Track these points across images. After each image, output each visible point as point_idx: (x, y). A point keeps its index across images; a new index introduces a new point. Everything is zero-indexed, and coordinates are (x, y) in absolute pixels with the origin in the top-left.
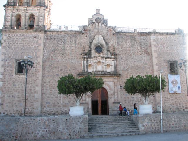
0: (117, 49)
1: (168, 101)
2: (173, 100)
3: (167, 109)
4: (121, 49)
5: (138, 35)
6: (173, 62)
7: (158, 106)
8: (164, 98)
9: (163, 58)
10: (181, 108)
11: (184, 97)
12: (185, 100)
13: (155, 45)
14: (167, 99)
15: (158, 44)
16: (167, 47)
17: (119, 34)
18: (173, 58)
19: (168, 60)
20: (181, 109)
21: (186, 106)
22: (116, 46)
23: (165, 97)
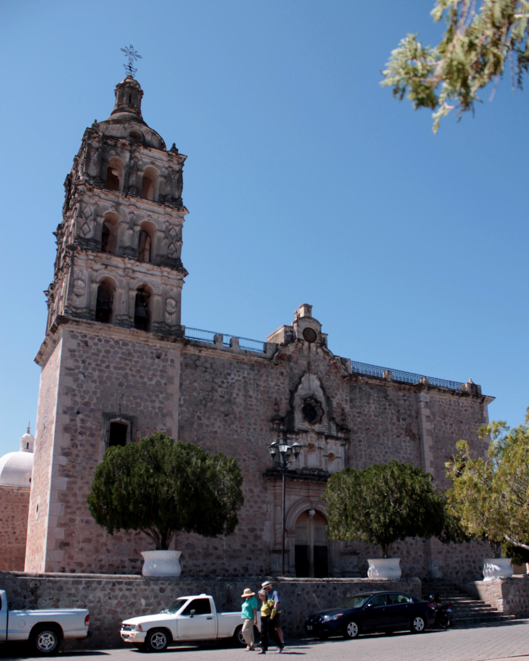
0: (350, 418)
1: (453, 553)
3: (451, 573)
4: (359, 417)
9: (444, 451)
15: (433, 414)
17: (354, 379)
22: (347, 407)
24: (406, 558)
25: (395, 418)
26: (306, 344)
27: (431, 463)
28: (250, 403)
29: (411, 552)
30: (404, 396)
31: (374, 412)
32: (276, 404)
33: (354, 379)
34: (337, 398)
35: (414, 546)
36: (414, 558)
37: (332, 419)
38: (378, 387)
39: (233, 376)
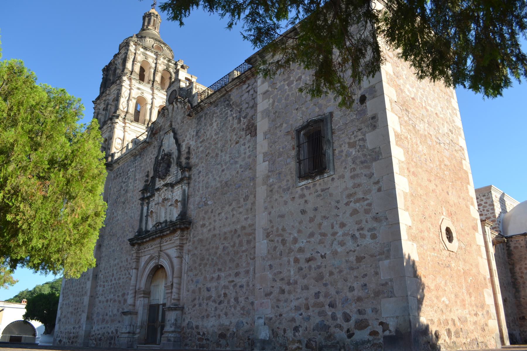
0: (193, 153)
1: (290, 292)
2: (306, 288)
4: (201, 147)
6: (315, 122)
7: (259, 318)
8: (279, 284)
9: (285, 125)
10: (336, 327)
11: (352, 269)
12: (355, 285)
13: (267, 91)
14: (289, 284)
16: (300, 78)
17: (199, 109)
18: (317, 110)
19: (300, 123)
20: (338, 330)
21: (360, 312)
22: (192, 143)
23: (282, 279)
24: (233, 309)
25: (236, 121)
26: (170, 108)
27: (265, 154)
29: (240, 299)
31: (215, 130)
32: (147, 176)
33: (199, 109)
34: (186, 139)
35: (244, 290)
36: (243, 308)
37: (179, 164)
38: (222, 99)
39: (131, 170)
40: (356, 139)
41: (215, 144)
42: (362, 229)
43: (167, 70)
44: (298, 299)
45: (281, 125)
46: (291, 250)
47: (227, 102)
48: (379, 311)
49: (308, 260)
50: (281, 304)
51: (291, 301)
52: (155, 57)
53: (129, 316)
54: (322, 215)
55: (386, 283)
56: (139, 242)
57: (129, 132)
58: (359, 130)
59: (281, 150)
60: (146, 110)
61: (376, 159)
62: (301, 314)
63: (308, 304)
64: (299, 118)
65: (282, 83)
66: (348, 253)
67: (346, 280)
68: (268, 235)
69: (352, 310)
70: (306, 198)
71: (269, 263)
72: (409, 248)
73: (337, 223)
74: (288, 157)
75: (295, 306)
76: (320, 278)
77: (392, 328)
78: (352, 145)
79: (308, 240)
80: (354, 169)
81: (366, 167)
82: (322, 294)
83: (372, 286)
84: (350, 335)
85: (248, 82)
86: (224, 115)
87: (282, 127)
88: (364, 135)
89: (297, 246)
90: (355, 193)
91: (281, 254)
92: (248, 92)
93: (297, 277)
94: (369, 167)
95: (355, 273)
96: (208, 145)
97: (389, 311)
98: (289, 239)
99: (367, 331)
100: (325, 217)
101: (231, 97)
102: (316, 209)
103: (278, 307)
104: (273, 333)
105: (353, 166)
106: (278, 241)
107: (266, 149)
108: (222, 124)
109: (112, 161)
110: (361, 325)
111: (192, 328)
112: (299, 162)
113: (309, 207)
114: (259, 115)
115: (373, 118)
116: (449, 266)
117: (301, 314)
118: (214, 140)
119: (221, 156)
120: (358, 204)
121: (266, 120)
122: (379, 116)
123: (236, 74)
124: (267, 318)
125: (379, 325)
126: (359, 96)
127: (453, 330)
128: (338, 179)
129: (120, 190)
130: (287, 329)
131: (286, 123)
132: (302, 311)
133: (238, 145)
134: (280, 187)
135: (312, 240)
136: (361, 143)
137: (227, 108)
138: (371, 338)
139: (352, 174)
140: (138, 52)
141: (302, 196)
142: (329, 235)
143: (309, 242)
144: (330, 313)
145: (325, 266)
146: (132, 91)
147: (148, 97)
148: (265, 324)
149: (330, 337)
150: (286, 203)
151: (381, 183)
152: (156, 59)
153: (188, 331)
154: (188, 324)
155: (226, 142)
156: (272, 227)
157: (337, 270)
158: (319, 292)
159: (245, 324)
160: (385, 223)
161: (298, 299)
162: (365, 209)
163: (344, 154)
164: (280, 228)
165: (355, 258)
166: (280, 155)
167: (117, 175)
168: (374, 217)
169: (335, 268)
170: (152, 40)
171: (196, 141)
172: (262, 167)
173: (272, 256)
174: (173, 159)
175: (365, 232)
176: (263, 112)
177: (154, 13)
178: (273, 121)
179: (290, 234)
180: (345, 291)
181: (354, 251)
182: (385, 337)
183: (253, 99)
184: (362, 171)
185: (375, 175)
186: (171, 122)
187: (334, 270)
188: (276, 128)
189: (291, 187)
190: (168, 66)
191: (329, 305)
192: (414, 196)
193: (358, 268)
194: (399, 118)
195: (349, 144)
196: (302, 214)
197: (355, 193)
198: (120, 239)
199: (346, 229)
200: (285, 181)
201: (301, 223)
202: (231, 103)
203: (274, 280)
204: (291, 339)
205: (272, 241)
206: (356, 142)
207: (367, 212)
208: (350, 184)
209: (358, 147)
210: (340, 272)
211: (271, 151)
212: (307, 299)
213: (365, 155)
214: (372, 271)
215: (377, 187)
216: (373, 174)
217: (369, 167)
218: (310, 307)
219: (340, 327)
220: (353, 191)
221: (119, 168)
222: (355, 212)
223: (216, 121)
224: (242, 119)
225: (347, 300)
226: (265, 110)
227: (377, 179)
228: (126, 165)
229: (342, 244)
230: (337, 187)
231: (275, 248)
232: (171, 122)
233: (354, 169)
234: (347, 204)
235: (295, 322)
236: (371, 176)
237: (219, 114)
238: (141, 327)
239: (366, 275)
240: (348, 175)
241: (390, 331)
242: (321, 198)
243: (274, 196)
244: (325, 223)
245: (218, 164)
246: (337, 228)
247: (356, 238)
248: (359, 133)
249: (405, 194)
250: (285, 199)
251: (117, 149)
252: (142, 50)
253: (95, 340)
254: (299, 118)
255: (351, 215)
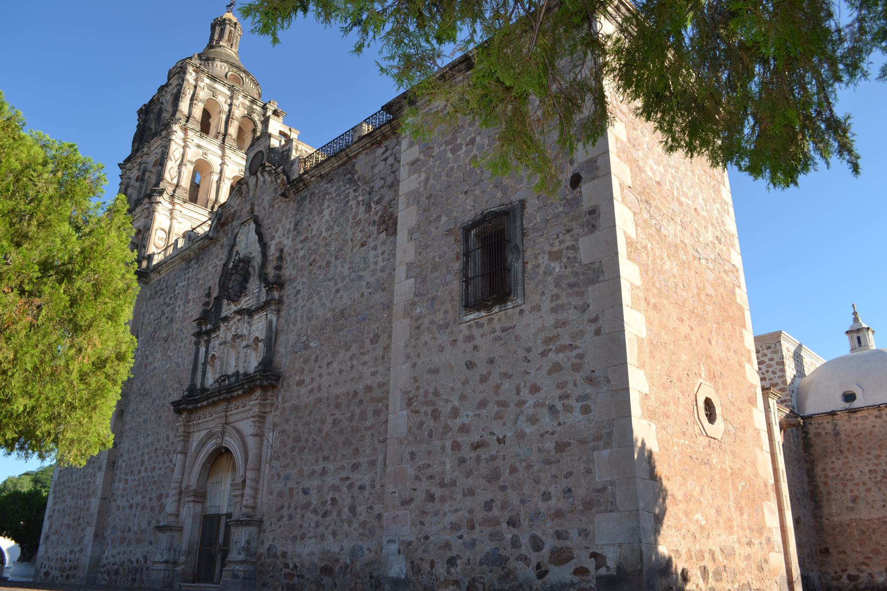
0: (288, 258)
1: (443, 500)
2: (471, 492)
3: (432, 564)
5: (365, 148)
6: (496, 215)
8: (425, 485)
9: (444, 219)
10: (518, 559)
11: (548, 462)
12: (552, 490)
13: (417, 160)
14: (442, 485)
15: (427, 149)
16: (473, 141)
17: (301, 184)
20: (521, 564)
21: (559, 535)
22: (287, 242)
23: (431, 477)
24: (346, 525)
25: (362, 208)
27: (410, 266)
28: (187, 310)
29: (359, 509)
30: (386, 150)
31: (327, 221)
32: (208, 295)
33: (301, 184)
34: (277, 235)
35: (366, 494)
36: (363, 524)
37: (263, 277)
38: (341, 170)
40: (563, 246)
41: (326, 245)
42: (567, 396)
43: (248, 117)
44: (456, 511)
45: (439, 218)
46: (447, 429)
47: (349, 176)
48: (591, 534)
49: (476, 446)
50: (428, 519)
51: (445, 514)
52: (229, 93)
53: (168, 533)
54: (502, 370)
55: (604, 488)
56: (190, 407)
57: (180, 219)
58: (568, 231)
59: (437, 259)
60: (210, 182)
61: (593, 281)
62: (461, 537)
63: (472, 520)
64: (469, 207)
65: (443, 148)
66: (542, 435)
67: (537, 482)
68: (409, 403)
69: (546, 531)
70: (475, 343)
71: (411, 448)
72: (644, 430)
73: (525, 386)
74: (449, 272)
75: (451, 523)
76: (494, 476)
77: (611, 563)
78: (555, 256)
79: (477, 412)
80: (557, 296)
81: (577, 294)
82: (497, 503)
83: (580, 492)
84: (542, 573)
85: (386, 143)
86: (342, 197)
87: (440, 221)
88: (576, 240)
89: (458, 421)
90: (558, 337)
91: (430, 435)
92: (385, 160)
93: (456, 474)
94: (581, 294)
95: (553, 470)
96: (314, 247)
97: (607, 537)
98: (446, 410)
99: (571, 566)
100: (506, 375)
101: (356, 168)
102: (491, 361)
103: (422, 523)
104: (413, 568)
105: (555, 291)
106: (426, 413)
107: (411, 257)
108: (339, 212)
109: (148, 267)
110: (561, 557)
111: (275, 556)
112: (467, 281)
113: (481, 357)
114: (402, 200)
115: (592, 212)
116: (707, 463)
117: (461, 537)
118: (325, 239)
119: (336, 267)
120: (561, 355)
121: (414, 208)
122: (602, 210)
123: (366, 129)
124: (402, 542)
125: (590, 557)
126: (570, 175)
127: (711, 569)
128: (530, 312)
129: (160, 318)
130: (436, 561)
131: (447, 215)
132: (462, 531)
133: (364, 248)
134: (432, 322)
135: (484, 412)
136: (571, 253)
137: (348, 186)
138: (576, 579)
139: (554, 304)
140: (201, 84)
141: (470, 338)
142: (512, 406)
143: (479, 416)
144: (509, 536)
145: (504, 456)
146: (188, 149)
147: (215, 161)
148: (399, 553)
149: (508, 576)
150: (441, 349)
151: (601, 321)
152: (231, 98)
153: (268, 561)
154: (269, 549)
155: (345, 242)
156: (418, 388)
157: (524, 464)
158: (492, 501)
159: (366, 552)
160: (605, 388)
161: (456, 511)
162: (573, 365)
163: (541, 270)
164: (431, 390)
165: (554, 445)
166: (435, 268)
167: (156, 292)
168: (587, 378)
169: (521, 461)
170: (226, 65)
171: (293, 240)
172: (404, 288)
173: (416, 438)
174: (254, 267)
175: (572, 402)
176: (408, 195)
177: (230, 20)
178: (424, 211)
179: (447, 401)
180: (536, 500)
181: (553, 434)
182: (599, 578)
183: (393, 172)
184: (570, 300)
185: (591, 308)
186: (253, 205)
187: (518, 465)
188: (430, 222)
189: (451, 324)
190: (251, 111)
191: (508, 523)
192: (653, 345)
193: (558, 461)
194: (635, 214)
195: (550, 253)
196: (468, 368)
197: (558, 337)
198: (158, 401)
199: (541, 395)
200: (442, 312)
201: (465, 382)
202: (356, 177)
203: (417, 478)
204: (442, 579)
205: (416, 412)
206: (561, 251)
207: (576, 368)
208: (550, 320)
209: (565, 260)
210: (529, 467)
211: (419, 261)
212: (471, 512)
213: (576, 274)
214: (582, 467)
215: (594, 327)
216: (588, 306)
217: (581, 294)
218: (476, 525)
219: (525, 559)
220: (555, 332)
221: (160, 280)
222: (556, 368)
223: (329, 206)
224: (373, 205)
225: (537, 514)
226: (413, 191)
227: (594, 315)
228: (172, 274)
229: (533, 420)
230: (528, 325)
231: (421, 424)
232: (253, 205)
233: (557, 296)
234: (544, 354)
235: (450, 549)
236: (584, 308)
237: (334, 195)
238: (189, 552)
239: (570, 474)
240: (546, 305)
241: (608, 567)
242: (501, 342)
243: (422, 337)
244: (506, 385)
245: (330, 280)
246: (525, 393)
247: (557, 412)
248: (568, 237)
249: (640, 341)
250: (440, 341)
251: (157, 248)
252: (207, 81)
253: (108, 573)
254: (469, 207)
255: (550, 372)
